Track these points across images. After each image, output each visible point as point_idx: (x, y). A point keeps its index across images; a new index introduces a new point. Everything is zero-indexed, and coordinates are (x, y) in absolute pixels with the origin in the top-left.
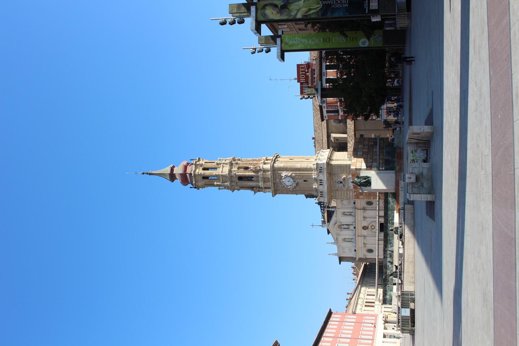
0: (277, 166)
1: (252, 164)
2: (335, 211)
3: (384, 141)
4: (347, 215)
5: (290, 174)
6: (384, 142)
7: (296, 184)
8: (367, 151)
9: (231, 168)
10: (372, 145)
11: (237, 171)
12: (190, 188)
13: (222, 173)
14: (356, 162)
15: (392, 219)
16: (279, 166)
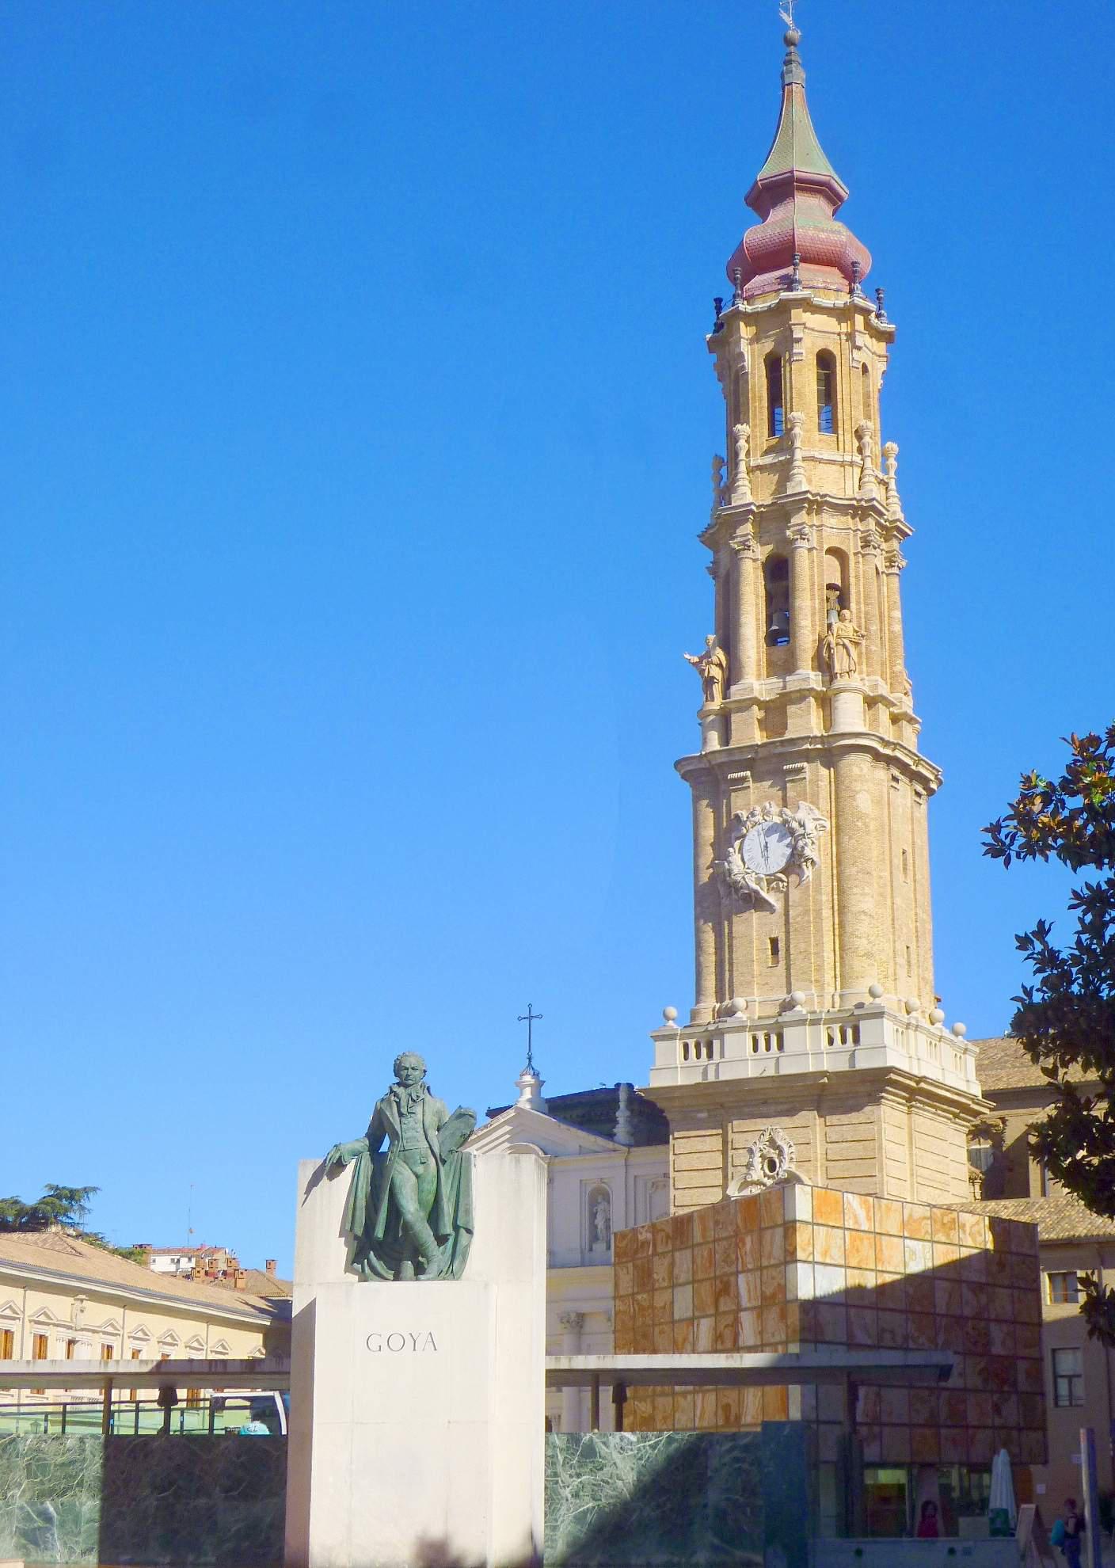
0: (856, 771)
1: (867, 629)
2: (610, 1145)
3: (1020, 1430)
4: (593, 1216)
5: (808, 852)
6: (1015, 1433)
7: (756, 892)
8: (941, 1308)
9: (840, 509)
10: (988, 1344)
11: (820, 541)
12: (718, 301)
13: (804, 459)
14: (850, 1224)
15: (76, 1521)
16: (857, 786)
